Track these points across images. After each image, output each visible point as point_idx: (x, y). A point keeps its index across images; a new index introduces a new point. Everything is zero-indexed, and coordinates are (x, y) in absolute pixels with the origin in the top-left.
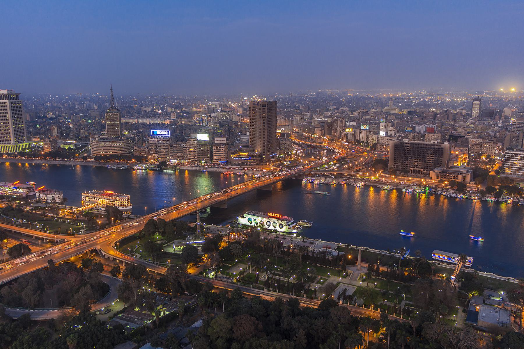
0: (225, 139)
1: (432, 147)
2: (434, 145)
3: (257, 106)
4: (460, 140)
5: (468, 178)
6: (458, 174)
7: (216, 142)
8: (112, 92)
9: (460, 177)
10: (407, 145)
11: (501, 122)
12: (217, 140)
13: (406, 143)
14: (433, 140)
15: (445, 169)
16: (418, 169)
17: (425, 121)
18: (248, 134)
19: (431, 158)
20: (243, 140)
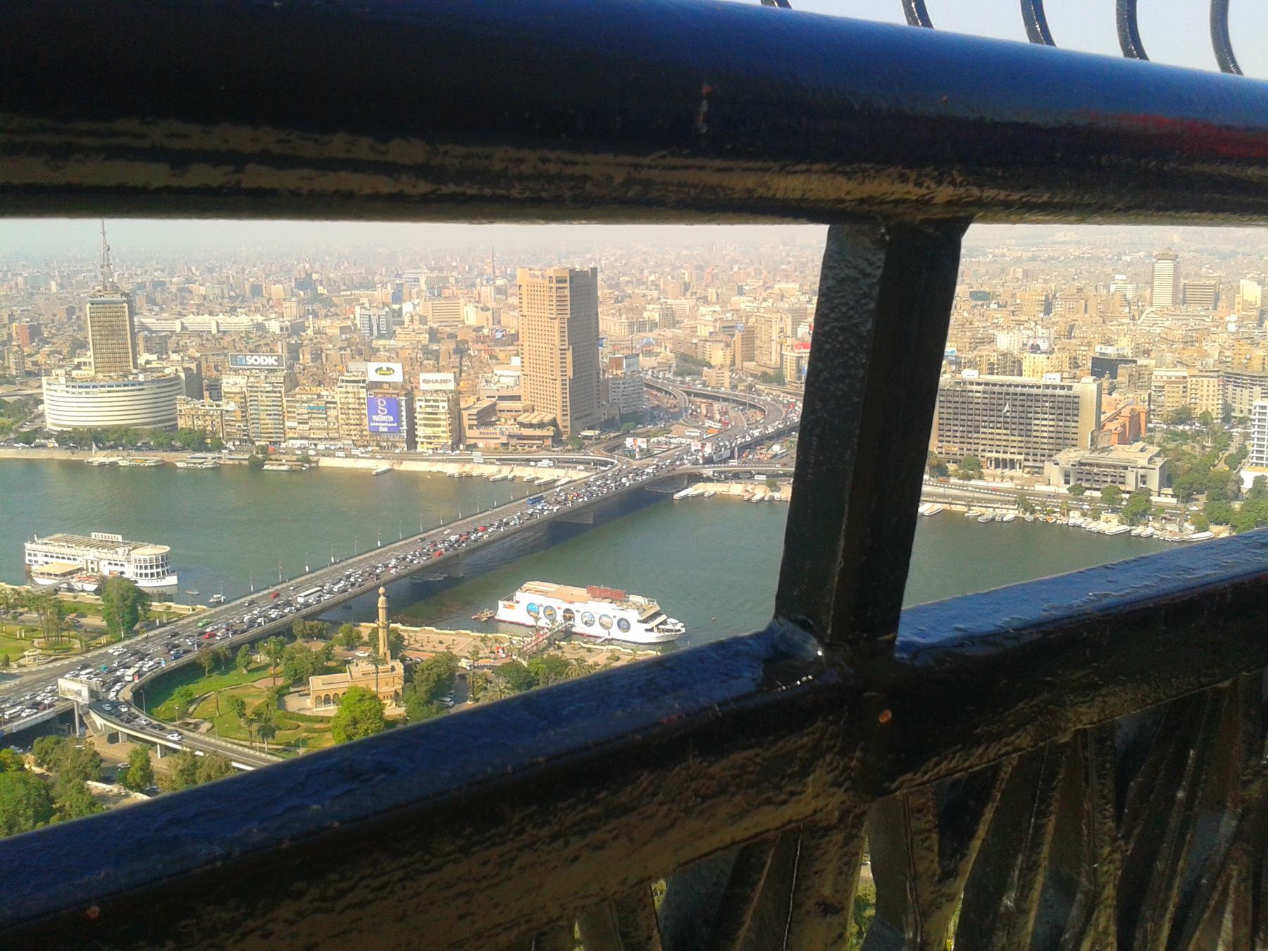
0: (450, 376)
1: (1049, 391)
2: (1055, 387)
3: (540, 280)
4: (1122, 371)
5: (1154, 483)
6: (1126, 468)
7: (423, 386)
8: (105, 242)
9: (1131, 477)
10: (975, 388)
11: (1234, 318)
12: (425, 381)
13: (972, 383)
14: (1039, 372)
15: (1087, 454)
16: (1008, 456)
17: (1023, 318)
18: (516, 361)
19: (1044, 425)
20: (502, 379)
